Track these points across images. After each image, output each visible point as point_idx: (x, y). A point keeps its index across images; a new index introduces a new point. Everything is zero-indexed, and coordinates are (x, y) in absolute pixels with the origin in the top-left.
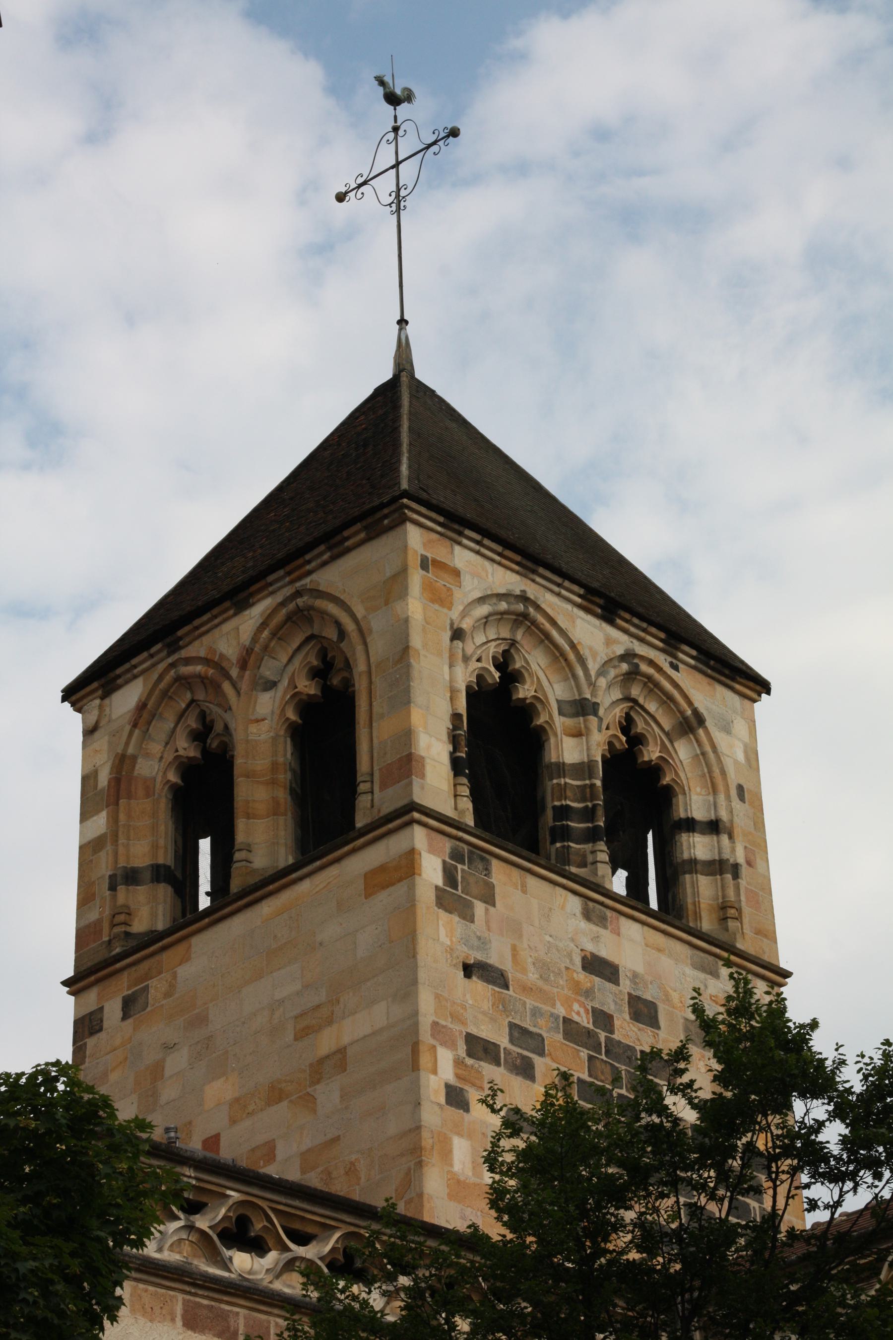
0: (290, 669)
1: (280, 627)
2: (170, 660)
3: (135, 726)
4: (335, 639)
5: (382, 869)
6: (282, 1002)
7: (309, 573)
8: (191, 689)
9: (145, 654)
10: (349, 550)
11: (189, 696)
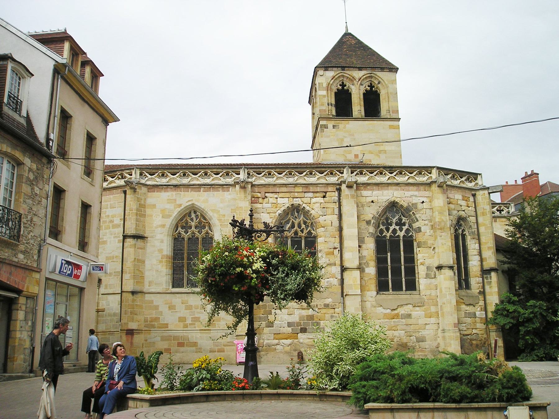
0: (366, 84)
1: (367, 77)
2: (342, 71)
4: (377, 83)
5: (393, 126)
6: (371, 139)
11: (342, 79)
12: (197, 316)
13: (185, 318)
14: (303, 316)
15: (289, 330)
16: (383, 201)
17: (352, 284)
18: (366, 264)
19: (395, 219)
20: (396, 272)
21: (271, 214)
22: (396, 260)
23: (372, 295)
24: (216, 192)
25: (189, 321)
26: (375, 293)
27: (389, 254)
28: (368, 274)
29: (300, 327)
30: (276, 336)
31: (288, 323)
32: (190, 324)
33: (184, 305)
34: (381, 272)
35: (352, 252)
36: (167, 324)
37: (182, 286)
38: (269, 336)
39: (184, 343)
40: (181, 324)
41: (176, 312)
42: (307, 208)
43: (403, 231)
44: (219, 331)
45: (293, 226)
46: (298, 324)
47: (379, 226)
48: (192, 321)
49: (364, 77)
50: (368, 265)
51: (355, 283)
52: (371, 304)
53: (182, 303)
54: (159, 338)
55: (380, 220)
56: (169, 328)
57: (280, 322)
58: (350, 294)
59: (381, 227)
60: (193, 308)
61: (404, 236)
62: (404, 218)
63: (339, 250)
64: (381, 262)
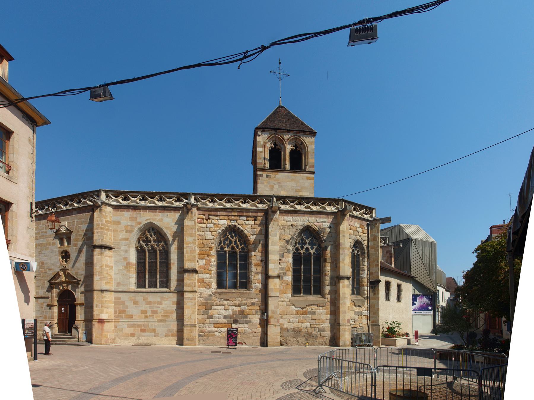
2: (275, 133)
3: (267, 139)
7: (299, 134)
8: (276, 138)
9: (271, 130)
10: (306, 134)
11: (275, 139)
12: (155, 309)
13: (146, 311)
14: (236, 311)
15: (225, 321)
16: (300, 225)
17: (273, 288)
18: (285, 274)
19: (308, 240)
20: (307, 281)
21: (212, 232)
22: (307, 271)
23: (288, 297)
24: (169, 213)
25: (149, 313)
26: (290, 295)
27: (302, 267)
28: (285, 281)
29: (233, 319)
30: (215, 325)
31: (224, 316)
32: (150, 315)
33: (145, 301)
34: (296, 280)
35: (274, 264)
36: (132, 315)
37: (145, 287)
38: (210, 325)
39: (145, 329)
40: (143, 316)
41: (139, 306)
42: (242, 228)
43: (314, 250)
44: (172, 321)
45: (231, 242)
46: (232, 317)
47: (295, 245)
48: (151, 313)
49: (291, 138)
50: (286, 274)
51: (276, 287)
52: (287, 303)
53: (144, 300)
54: (126, 326)
55: (297, 240)
56: (134, 319)
57: (218, 315)
58: (271, 295)
59: (298, 245)
60: (152, 303)
61: (314, 253)
62: (315, 240)
63: (264, 262)
64: (296, 271)
